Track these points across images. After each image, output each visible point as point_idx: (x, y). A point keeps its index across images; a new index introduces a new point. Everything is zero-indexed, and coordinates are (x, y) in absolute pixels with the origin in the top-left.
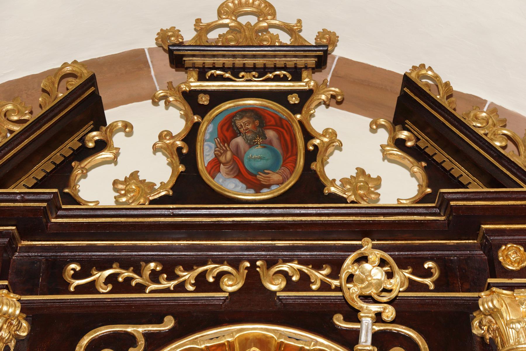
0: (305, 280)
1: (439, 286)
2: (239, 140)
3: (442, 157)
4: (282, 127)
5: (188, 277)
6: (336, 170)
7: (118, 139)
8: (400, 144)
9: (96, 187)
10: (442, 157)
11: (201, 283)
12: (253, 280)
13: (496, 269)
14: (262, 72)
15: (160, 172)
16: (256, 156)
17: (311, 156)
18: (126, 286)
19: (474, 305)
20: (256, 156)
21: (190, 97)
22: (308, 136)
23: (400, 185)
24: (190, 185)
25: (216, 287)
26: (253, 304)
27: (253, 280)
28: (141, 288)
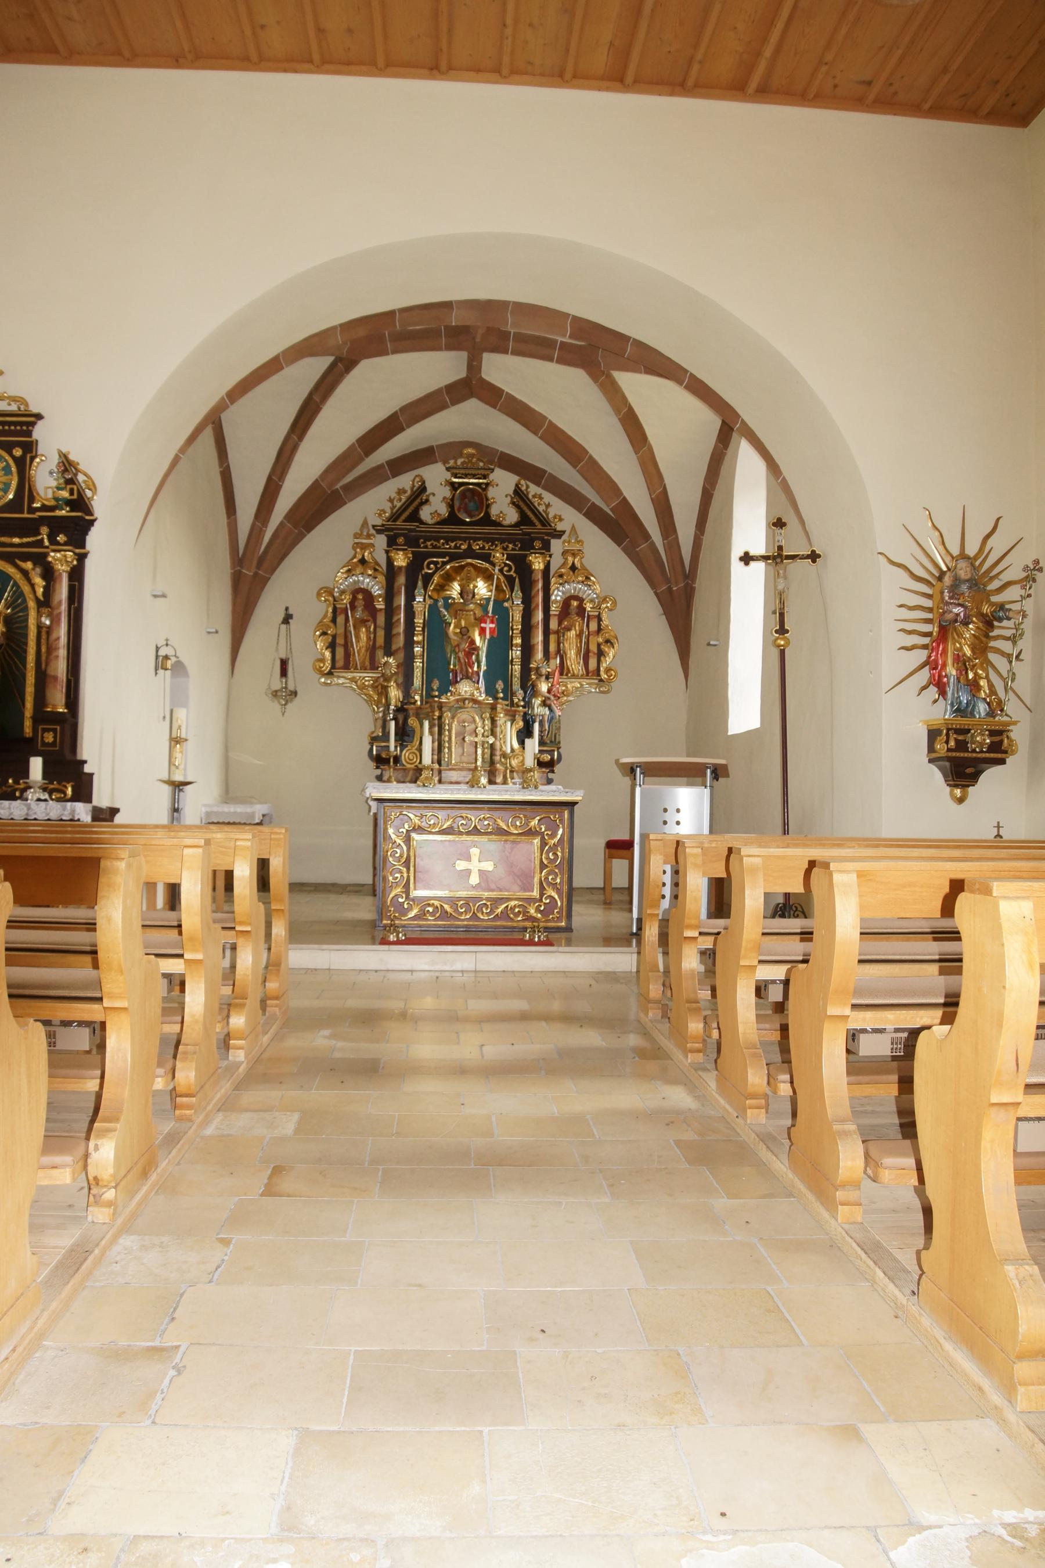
0: (483, 548)
1: (521, 549)
2: (467, 500)
3: (525, 508)
4: (479, 495)
5: (453, 544)
6: (494, 511)
7: (431, 498)
8: (513, 503)
9: (425, 514)
10: (525, 508)
11: (456, 547)
12: (470, 546)
13: (533, 548)
14: (474, 476)
15: (444, 511)
16: (471, 505)
17: (488, 506)
18: (435, 547)
19: (526, 556)
20: (471, 505)
21: (452, 484)
22: (487, 500)
23: (511, 516)
24: (452, 519)
25: (459, 548)
26: (470, 553)
27: (470, 546)
28: (439, 548)
